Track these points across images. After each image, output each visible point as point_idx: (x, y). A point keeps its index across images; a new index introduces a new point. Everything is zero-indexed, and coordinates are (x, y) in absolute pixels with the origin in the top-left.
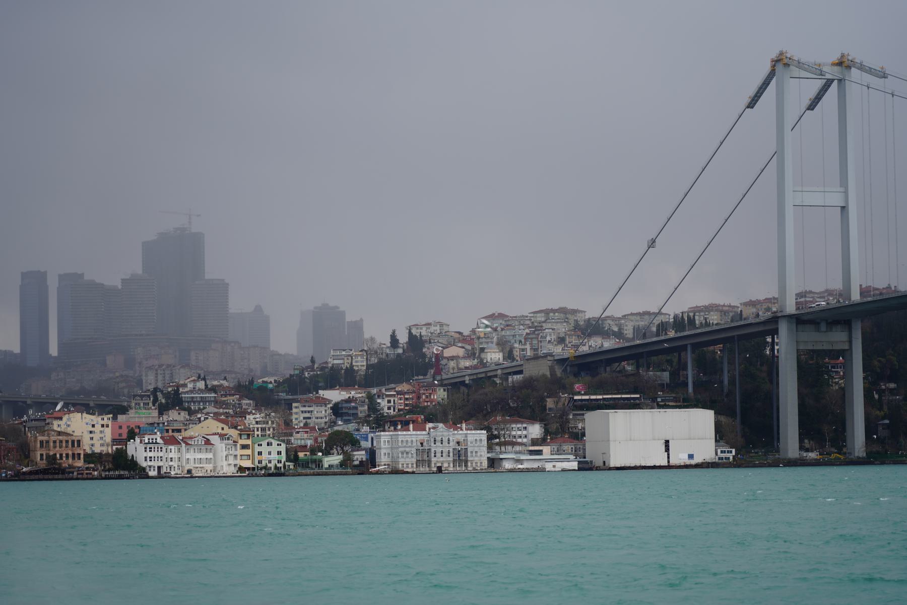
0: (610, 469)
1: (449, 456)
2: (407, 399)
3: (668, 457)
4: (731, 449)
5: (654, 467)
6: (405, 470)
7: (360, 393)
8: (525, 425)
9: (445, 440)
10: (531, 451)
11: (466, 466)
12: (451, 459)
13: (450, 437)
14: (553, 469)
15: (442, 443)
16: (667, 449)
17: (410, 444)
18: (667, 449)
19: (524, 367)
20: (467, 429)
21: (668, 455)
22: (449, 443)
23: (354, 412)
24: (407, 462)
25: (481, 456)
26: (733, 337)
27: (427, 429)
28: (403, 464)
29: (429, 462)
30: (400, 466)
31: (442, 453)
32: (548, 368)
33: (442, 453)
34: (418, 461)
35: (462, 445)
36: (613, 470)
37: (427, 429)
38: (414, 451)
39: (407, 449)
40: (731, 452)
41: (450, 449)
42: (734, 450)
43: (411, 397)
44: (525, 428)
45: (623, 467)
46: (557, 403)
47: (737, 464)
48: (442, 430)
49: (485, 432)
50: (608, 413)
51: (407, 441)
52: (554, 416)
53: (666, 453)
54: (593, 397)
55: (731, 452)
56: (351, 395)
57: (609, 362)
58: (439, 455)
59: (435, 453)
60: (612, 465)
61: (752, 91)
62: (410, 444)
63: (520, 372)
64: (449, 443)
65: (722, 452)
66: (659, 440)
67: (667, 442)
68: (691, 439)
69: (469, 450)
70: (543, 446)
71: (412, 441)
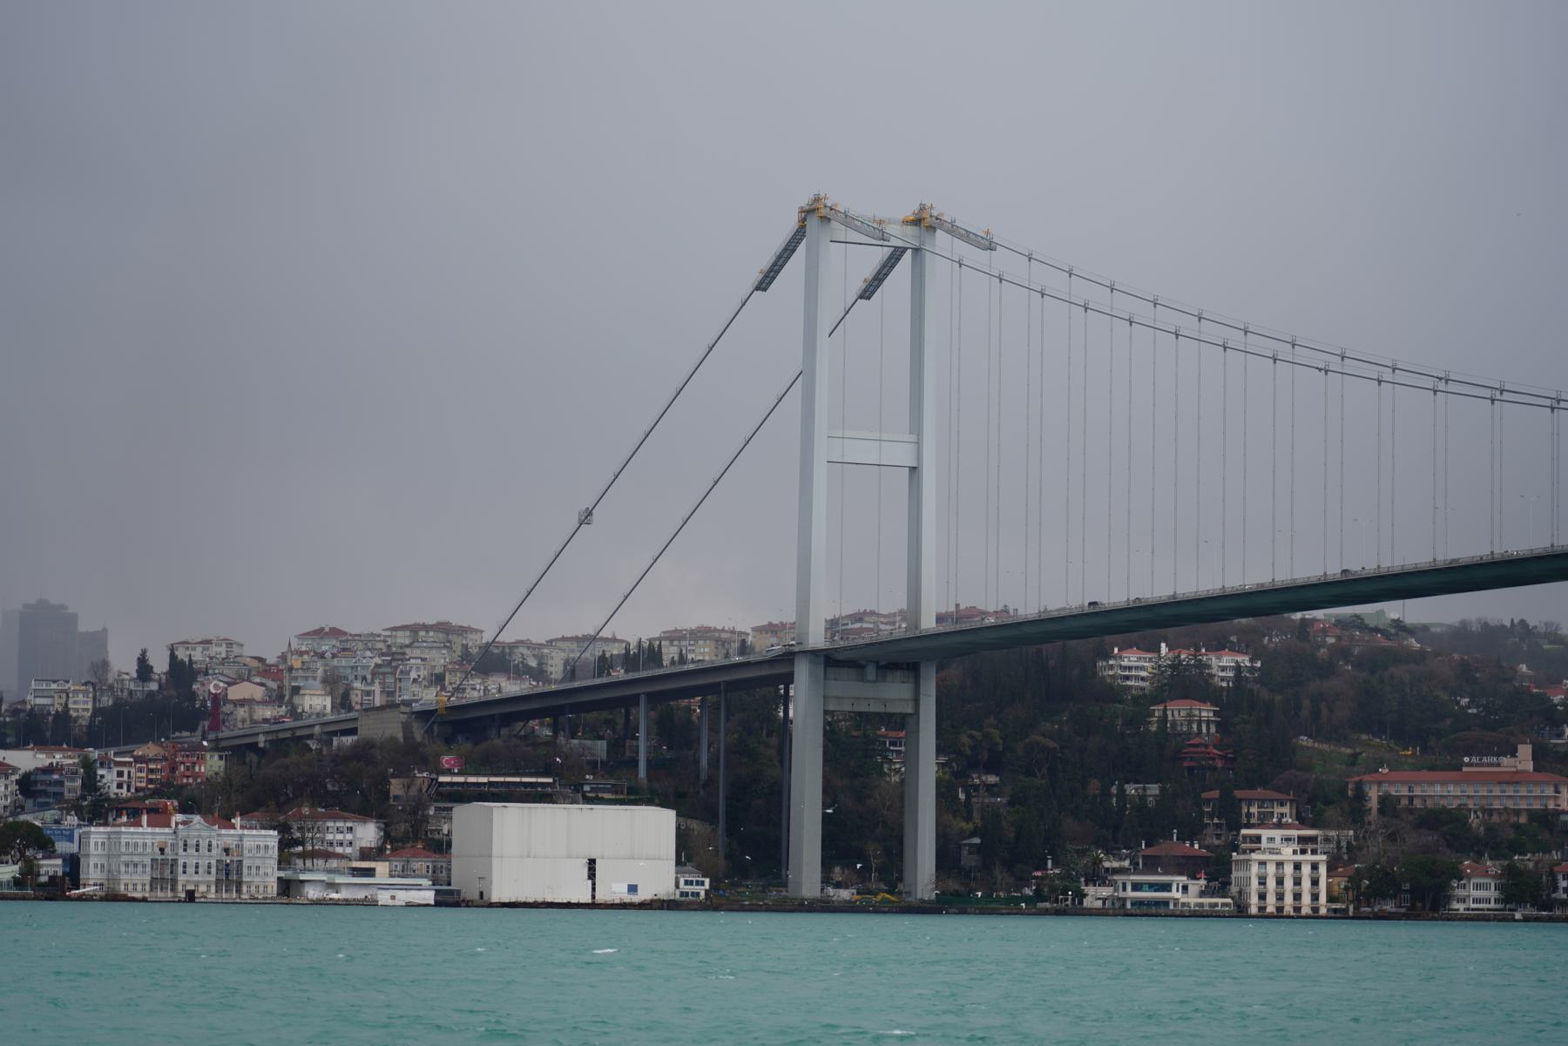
0: (491, 905)
1: (209, 873)
2: (152, 771)
3: (594, 889)
4: (702, 879)
5: (569, 905)
6: (129, 895)
7: (70, 757)
8: (349, 824)
9: (204, 844)
10: (354, 869)
11: (239, 891)
12: (213, 878)
13: (213, 840)
14: (390, 902)
15: (197, 850)
16: (592, 875)
17: (140, 850)
18: (592, 875)
19: (359, 723)
20: (242, 827)
21: (594, 884)
22: (210, 850)
23: (57, 789)
24: (135, 881)
25: (266, 874)
26: (718, 684)
27: (173, 825)
28: (126, 885)
29: (174, 881)
30: (122, 887)
31: (197, 867)
32: (400, 725)
33: (197, 867)
34: (153, 880)
35: (233, 855)
36: (497, 907)
37: (173, 825)
38: (147, 861)
39: (136, 859)
40: (702, 883)
41: (212, 862)
42: (707, 881)
43: (159, 767)
44: (350, 829)
45: (515, 903)
46: (409, 788)
47: (711, 904)
48: (198, 826)
49: (276, 833)
50: (491, 808)
51: (136, 845)
52: (402, 810)
53: (590, 882)
54: (472, 779)
55: (702, 883)
56: (54, 761)
57: (508, 719)
58: (191, 870)
59: (185, 866)
60: (495, 899)
61: (765, 262)
62: (140, 850)
63: (353, 731)
64: (210, 850)
65: (686, 883)
66: (578, 857)
67: (592, 862)
68: (633, 858)
69: (246, 863)
70: (377, 861)
71: (145, 845)
